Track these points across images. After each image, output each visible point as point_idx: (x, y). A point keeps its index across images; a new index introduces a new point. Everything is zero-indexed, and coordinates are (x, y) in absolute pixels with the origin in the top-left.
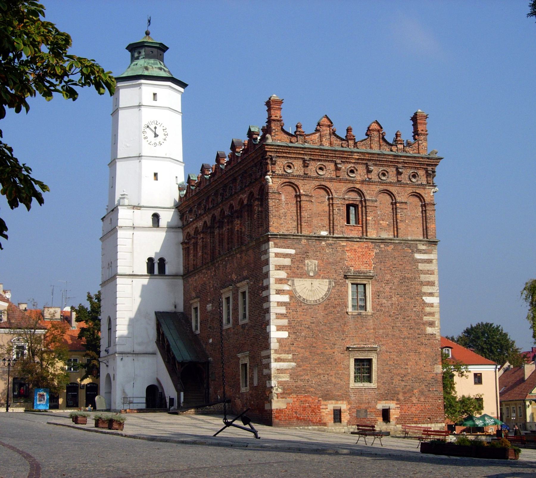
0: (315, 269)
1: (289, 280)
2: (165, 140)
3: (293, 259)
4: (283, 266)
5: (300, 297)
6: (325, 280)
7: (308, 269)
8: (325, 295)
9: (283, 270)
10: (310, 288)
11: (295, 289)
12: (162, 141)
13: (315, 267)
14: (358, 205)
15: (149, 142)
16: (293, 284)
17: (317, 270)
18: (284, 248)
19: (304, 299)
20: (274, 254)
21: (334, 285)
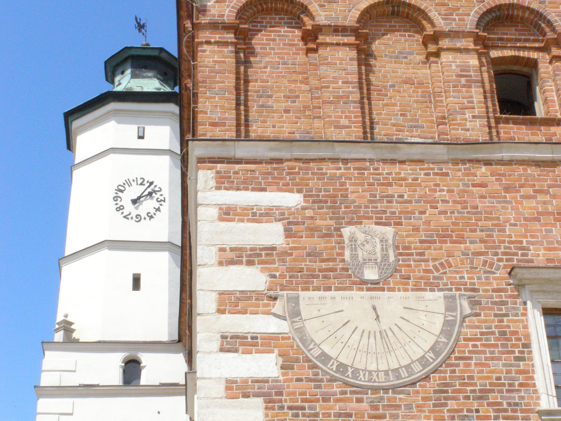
0: (385, 257)
1: (275, 299)
2: (158, 210)
3: (290, 223)
4: (252, 249)
5: (325, 357)
6: (428, 295)
7: (354, 257)
8: (432, 349)
9: (250, 263)
10: (369, 324)
11: (301, 331)
12: (152, 211)
13: (384, 249)
14: (533, 64)
15: (125, 214)
16: (295, 313)
17: (392, 258)
18: (253, 190)
19: (342, 368)
20: (214, 212)
21: (468, 311)
